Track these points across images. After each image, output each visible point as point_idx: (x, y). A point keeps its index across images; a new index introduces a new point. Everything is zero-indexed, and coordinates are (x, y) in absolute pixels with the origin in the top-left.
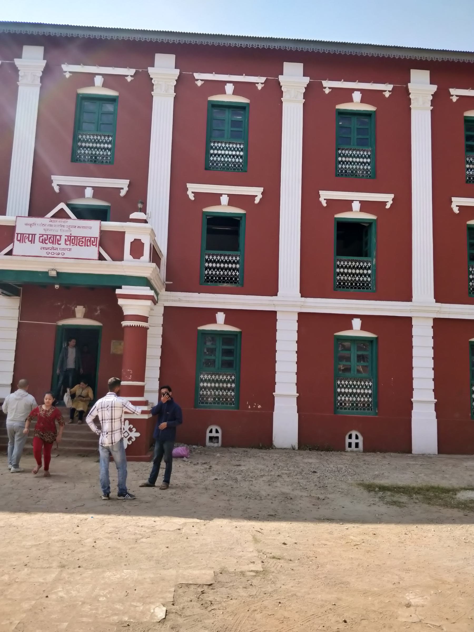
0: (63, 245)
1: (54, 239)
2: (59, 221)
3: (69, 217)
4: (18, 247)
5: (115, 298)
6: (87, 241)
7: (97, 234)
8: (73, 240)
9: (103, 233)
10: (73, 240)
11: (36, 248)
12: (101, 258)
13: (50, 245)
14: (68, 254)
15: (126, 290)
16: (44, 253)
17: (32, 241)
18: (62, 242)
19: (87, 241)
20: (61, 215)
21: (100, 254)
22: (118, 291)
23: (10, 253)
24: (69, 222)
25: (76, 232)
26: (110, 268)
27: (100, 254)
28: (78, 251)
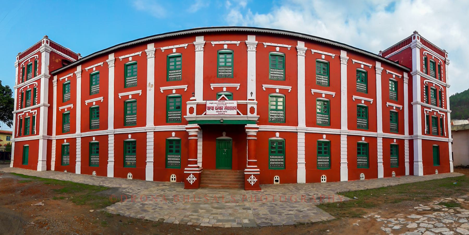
0: (224, 110)
1: (221, 108)
2: (222, 102)
3: (226, 100)
4: (208, 112)
5: (245, 129)
6: (233, 108)
7: (236, 106)
8: (227, 108)
9: (238, 105)
10: (227, 108)
11: (214, 112)
12: (238, 114)
13: (219, 110)
14: (226, 113)
15: (248, 126)
16: (217, 113)
17: (213, 109)
18: (224, 109)
19: (233, 108)
20: (223, 99)
21: (237, 112)
22: (246, 126)
23: (205, 114)
24: (226, 102)
25: (228, 105)
26: (242, 117)
27: (237, 112)
28: (230, 112)
